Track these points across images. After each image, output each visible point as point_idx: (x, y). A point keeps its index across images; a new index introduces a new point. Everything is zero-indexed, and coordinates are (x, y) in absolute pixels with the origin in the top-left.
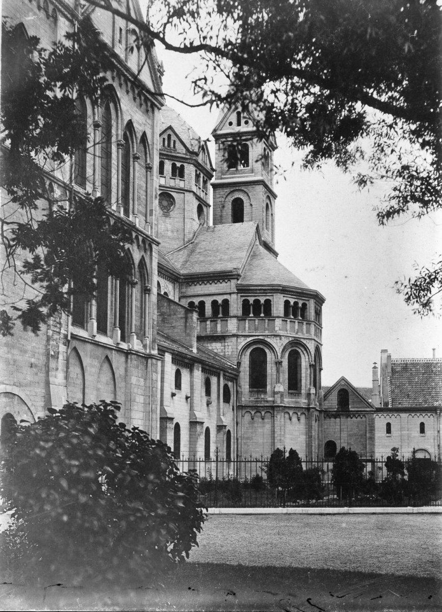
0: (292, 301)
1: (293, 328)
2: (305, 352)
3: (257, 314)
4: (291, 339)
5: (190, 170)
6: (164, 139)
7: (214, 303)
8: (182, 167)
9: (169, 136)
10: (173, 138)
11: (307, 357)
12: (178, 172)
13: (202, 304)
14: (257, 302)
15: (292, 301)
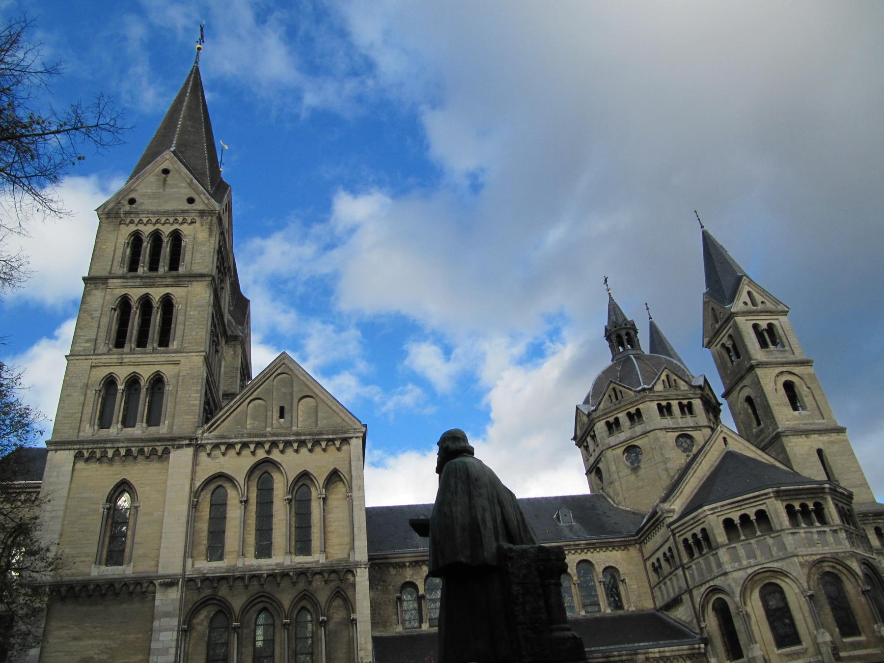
0: (735, 516)
1: (751, 555)
2: (787, 580)
3: (700, 549)
4: (750, 571)
5: (650, 408)
6: (610, 396)
7: (665, 554)
8: (638, 410)
9: (614, 389)
10: (619, 388)
11: (794, 586)
12: (635, 417)
13: (658, 560)
14: (694, 536)
15: (735, 516)
